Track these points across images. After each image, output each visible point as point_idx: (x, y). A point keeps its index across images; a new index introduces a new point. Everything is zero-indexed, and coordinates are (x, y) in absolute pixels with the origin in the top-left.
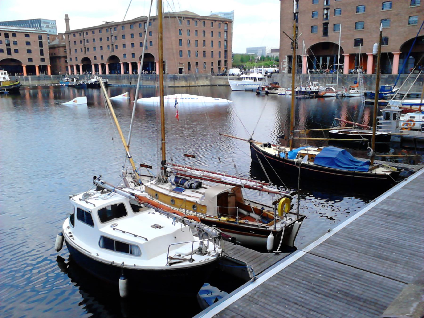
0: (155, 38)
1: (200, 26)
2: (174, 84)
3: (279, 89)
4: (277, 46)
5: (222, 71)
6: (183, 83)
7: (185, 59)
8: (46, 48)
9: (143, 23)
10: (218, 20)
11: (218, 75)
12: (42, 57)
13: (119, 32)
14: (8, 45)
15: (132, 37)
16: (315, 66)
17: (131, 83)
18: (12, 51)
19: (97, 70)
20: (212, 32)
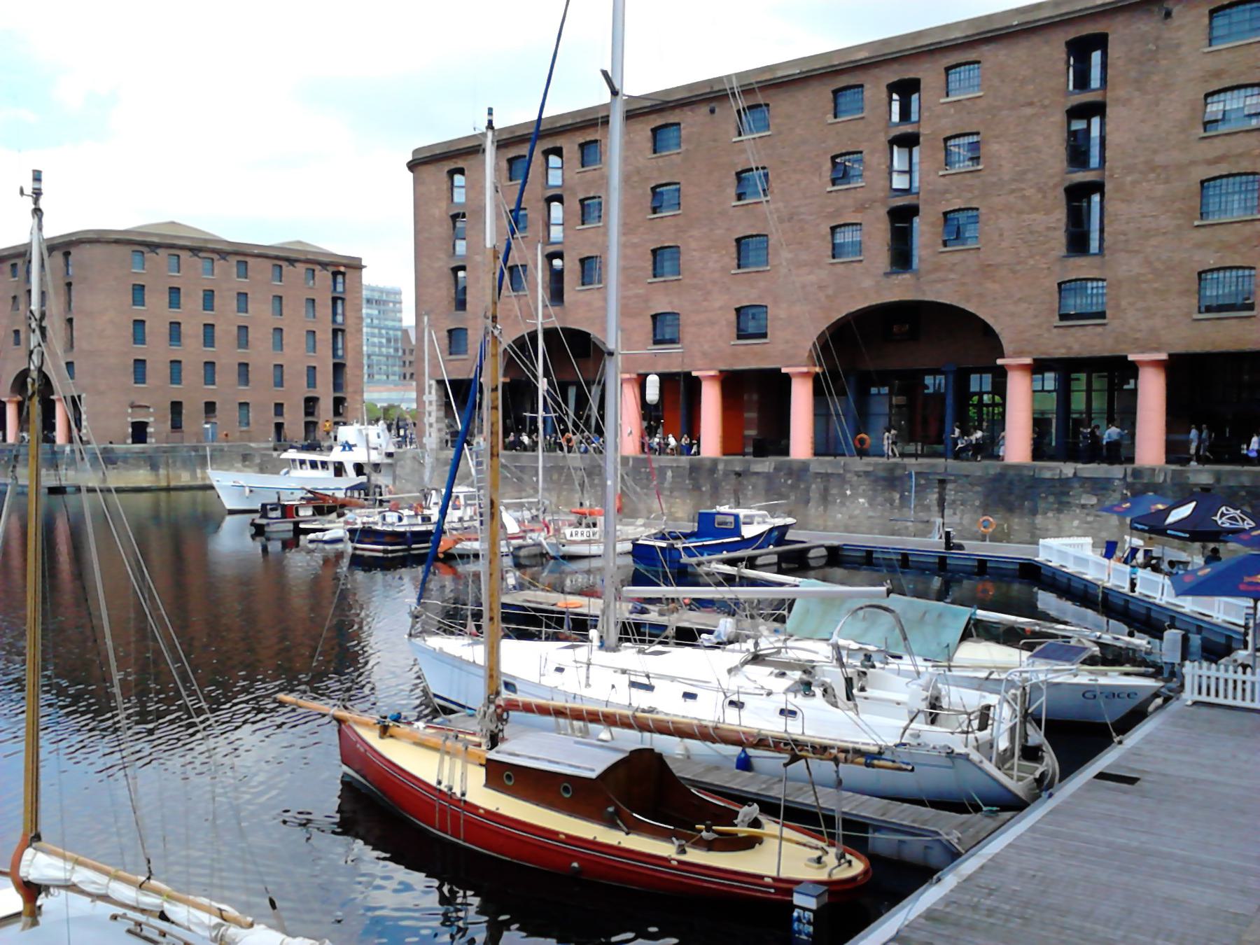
1: (225, 278)
10: (303, 257)
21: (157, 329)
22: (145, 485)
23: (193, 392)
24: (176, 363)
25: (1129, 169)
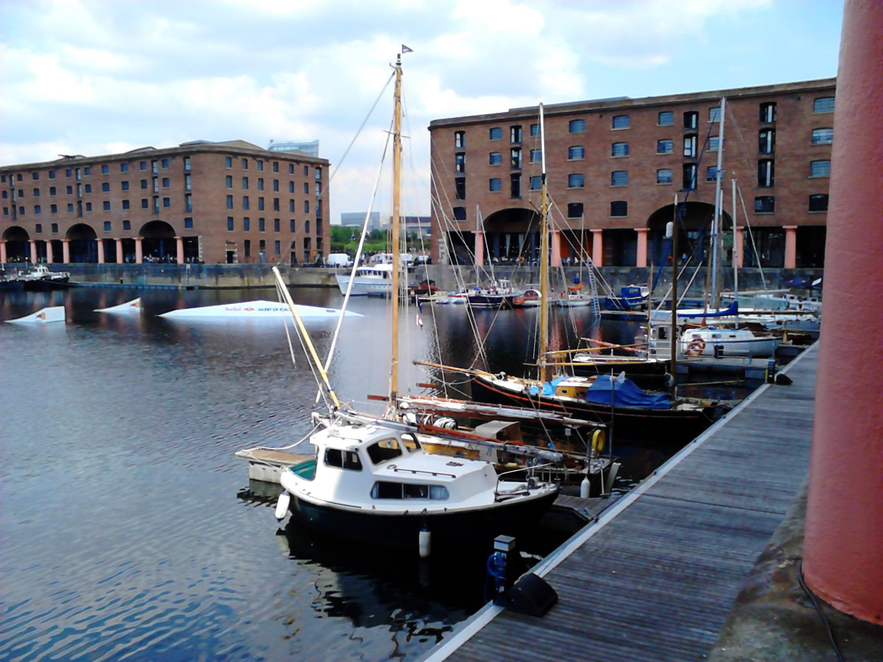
0: (175, 190)
2: (217, 283)
3: (437, 293)
4: (428, 214)
5: (311, 257)
6: (236, 281)
7: (238, 235)
9: (149, 162)
11: (305, 266)
13: (95, 177)
15: (123, 189)
16: (497, 252)
17: (122, 281)
19: (42, 253)
20: (292, 183)
21: (238, 200)
22: (238, 285)
23: (254, 234)
24: (247, 219)
25: (784, 156)
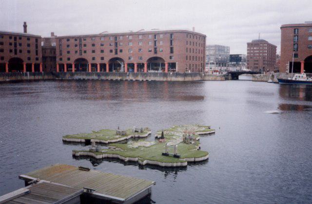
8: (40, 49)
12: (36, 56)
14: (15, 46)
18: (18, 51)
